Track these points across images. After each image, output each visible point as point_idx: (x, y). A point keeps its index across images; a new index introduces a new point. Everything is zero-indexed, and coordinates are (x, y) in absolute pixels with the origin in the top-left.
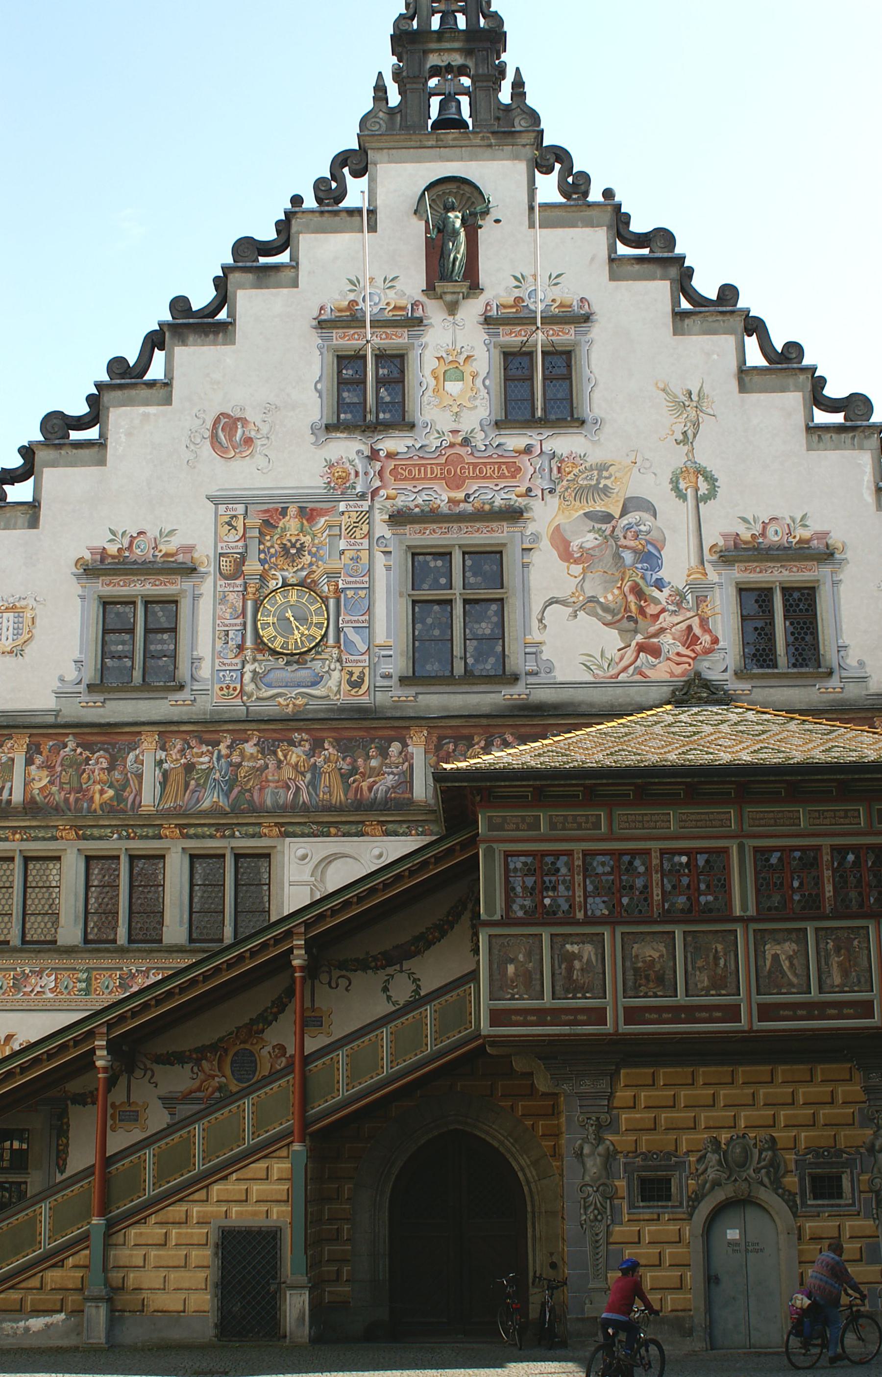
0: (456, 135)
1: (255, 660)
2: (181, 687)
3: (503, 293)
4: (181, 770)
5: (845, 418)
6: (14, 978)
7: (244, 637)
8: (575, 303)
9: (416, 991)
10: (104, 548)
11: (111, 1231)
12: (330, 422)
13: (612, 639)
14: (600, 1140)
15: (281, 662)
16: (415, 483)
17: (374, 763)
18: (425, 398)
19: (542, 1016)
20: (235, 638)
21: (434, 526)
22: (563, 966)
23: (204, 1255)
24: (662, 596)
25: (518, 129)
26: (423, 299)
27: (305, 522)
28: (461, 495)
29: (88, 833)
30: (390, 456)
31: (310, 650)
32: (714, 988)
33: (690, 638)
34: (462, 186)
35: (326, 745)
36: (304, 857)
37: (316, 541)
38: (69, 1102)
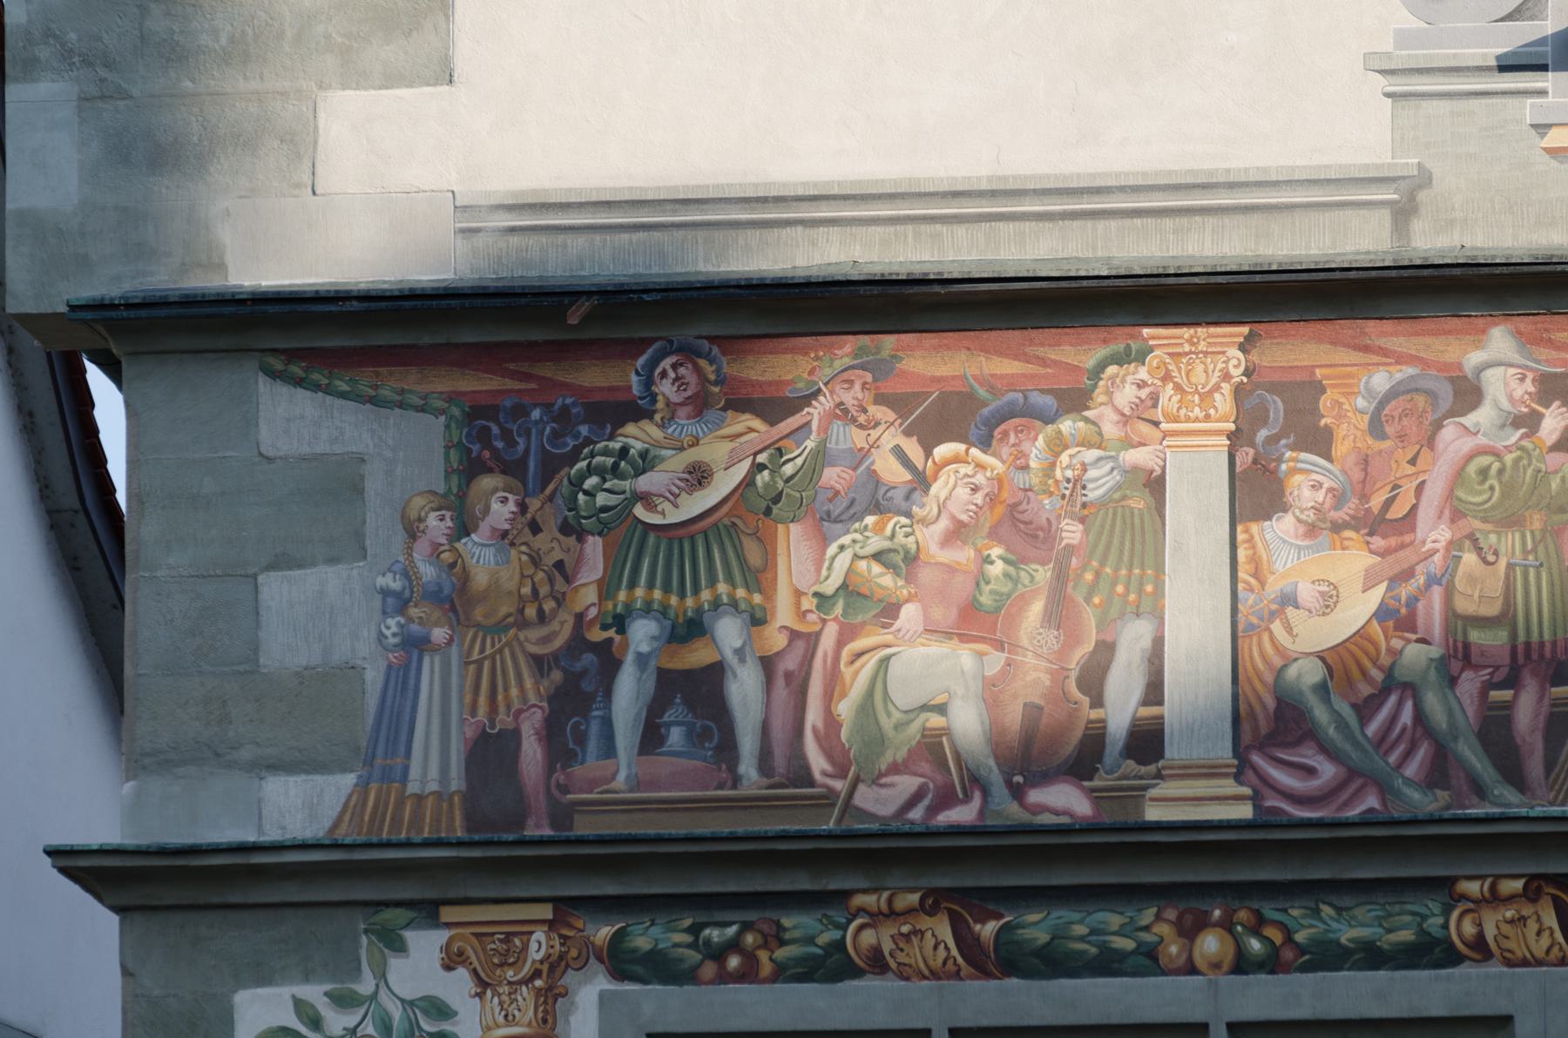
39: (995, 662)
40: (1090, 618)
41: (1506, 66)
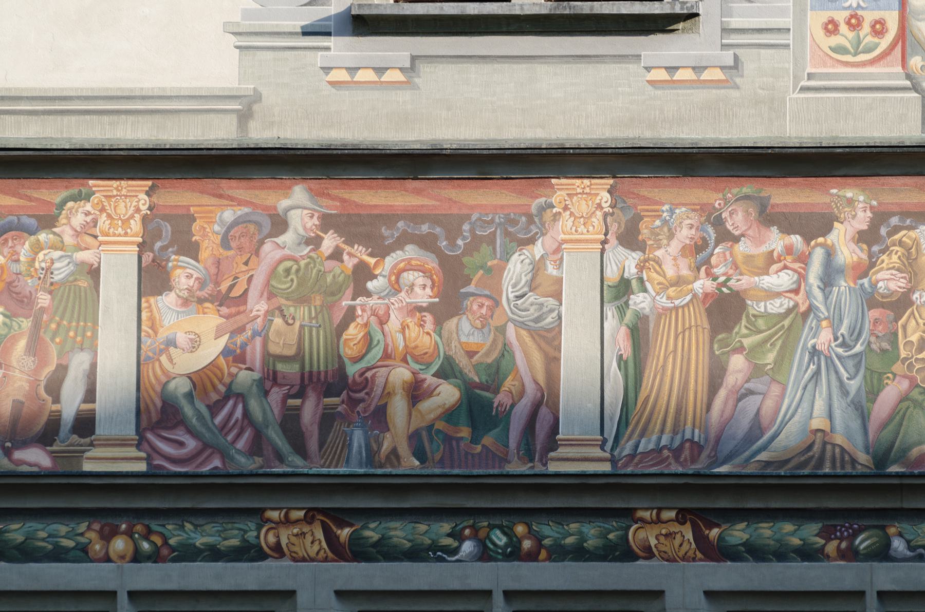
4: (698, 319)
29: (372, 533)
40: (54, 351)
41: (307, 33)
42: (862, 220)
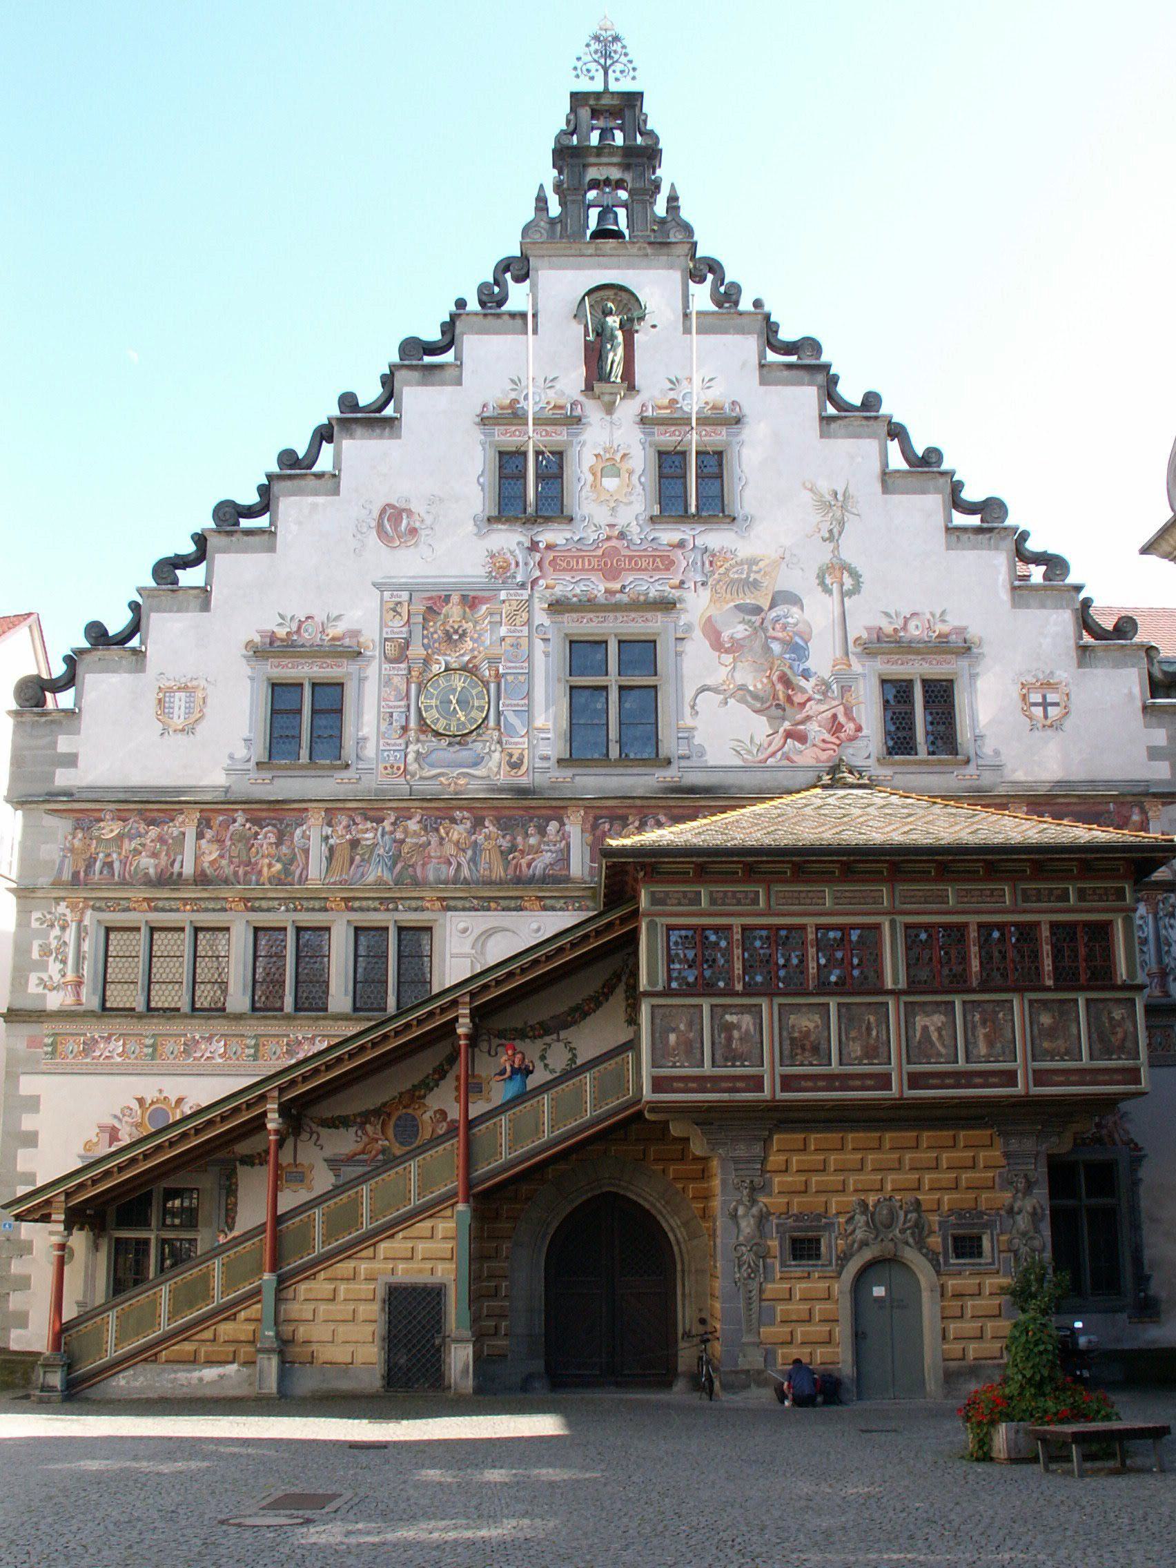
0: (613, 245)
1: (418, 741)
2: (347, 766)
3: (657, 394)
5: (982, 521)
6: (185, 1044)
7: (407, 718)
8: (727, 406)
9: (573, 1059)
10: (273, 632)
11: (281, 1287)
12: (493, 514)
13: (760, 727)
14: (753, 1202)
15: (444, 743)
16: (573, 573)
17: (532, 841)
18: (584, 493)
19: (702, 1083)
20: (398, 720)
21: (591, 615)
22: (723, 1036)
23: (373, 1310)
24: (809, 685)
25: (673, 240)
26: (582, 398)
27: (467, 609)
28: (618, 586)
29: (257, 904)
30: (549, 547)
31: (472, 732)
32: (868, 1058)
33: (835, 726)
34: (620, 293)
35: (487, 823)
36: (465, 930)
37: (478, 628)
38: (238, 1163)
39: (157, 861)
42: (392, 819)
